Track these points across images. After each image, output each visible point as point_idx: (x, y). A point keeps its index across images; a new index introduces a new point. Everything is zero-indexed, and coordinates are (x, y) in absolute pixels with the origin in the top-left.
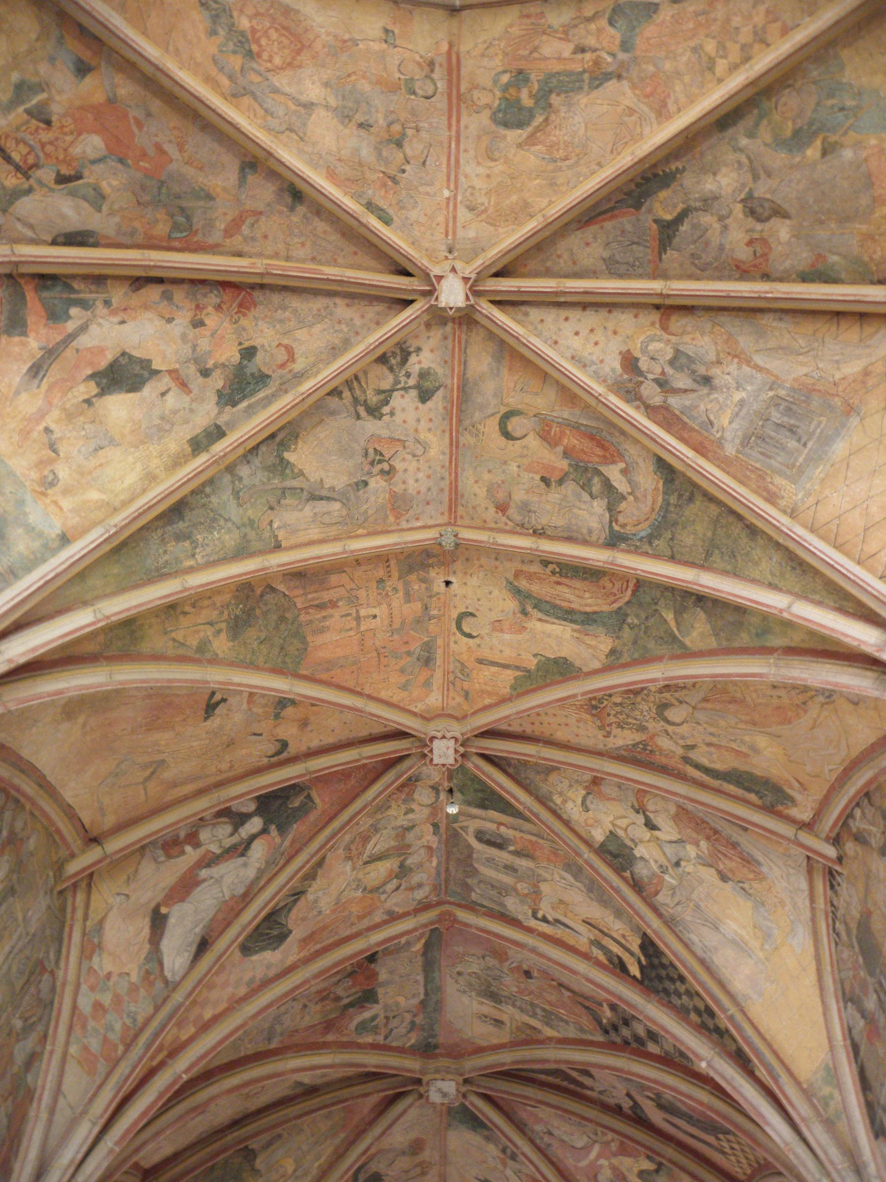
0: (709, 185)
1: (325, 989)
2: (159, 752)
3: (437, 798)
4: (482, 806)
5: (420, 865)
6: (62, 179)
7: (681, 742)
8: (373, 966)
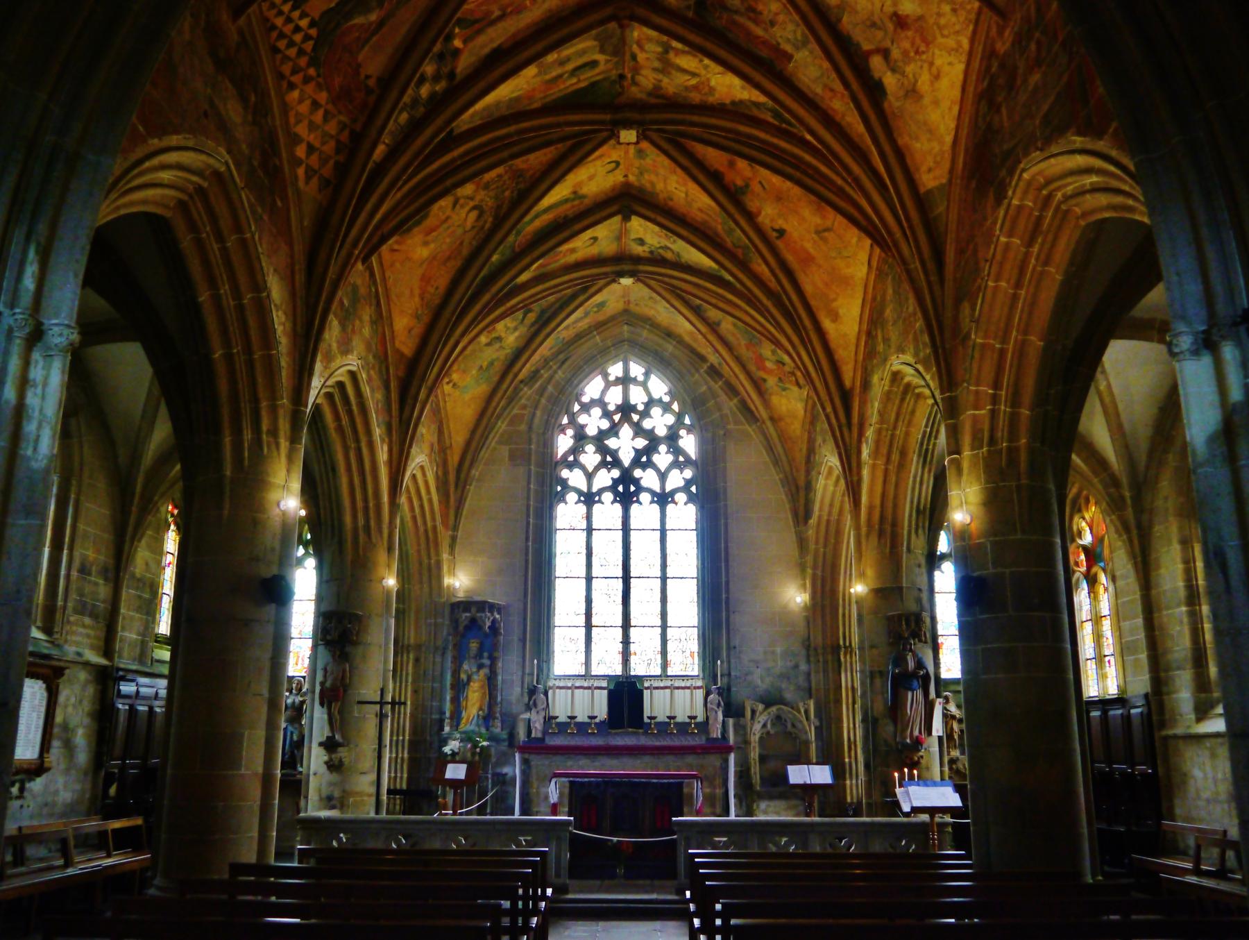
0: (517, 334)
1: (750, 18)
2: (815, 242)
3: (633, 78)
4: (593, 85)
5: (650, 39)
6: (784, 364)
7: (462, 201)
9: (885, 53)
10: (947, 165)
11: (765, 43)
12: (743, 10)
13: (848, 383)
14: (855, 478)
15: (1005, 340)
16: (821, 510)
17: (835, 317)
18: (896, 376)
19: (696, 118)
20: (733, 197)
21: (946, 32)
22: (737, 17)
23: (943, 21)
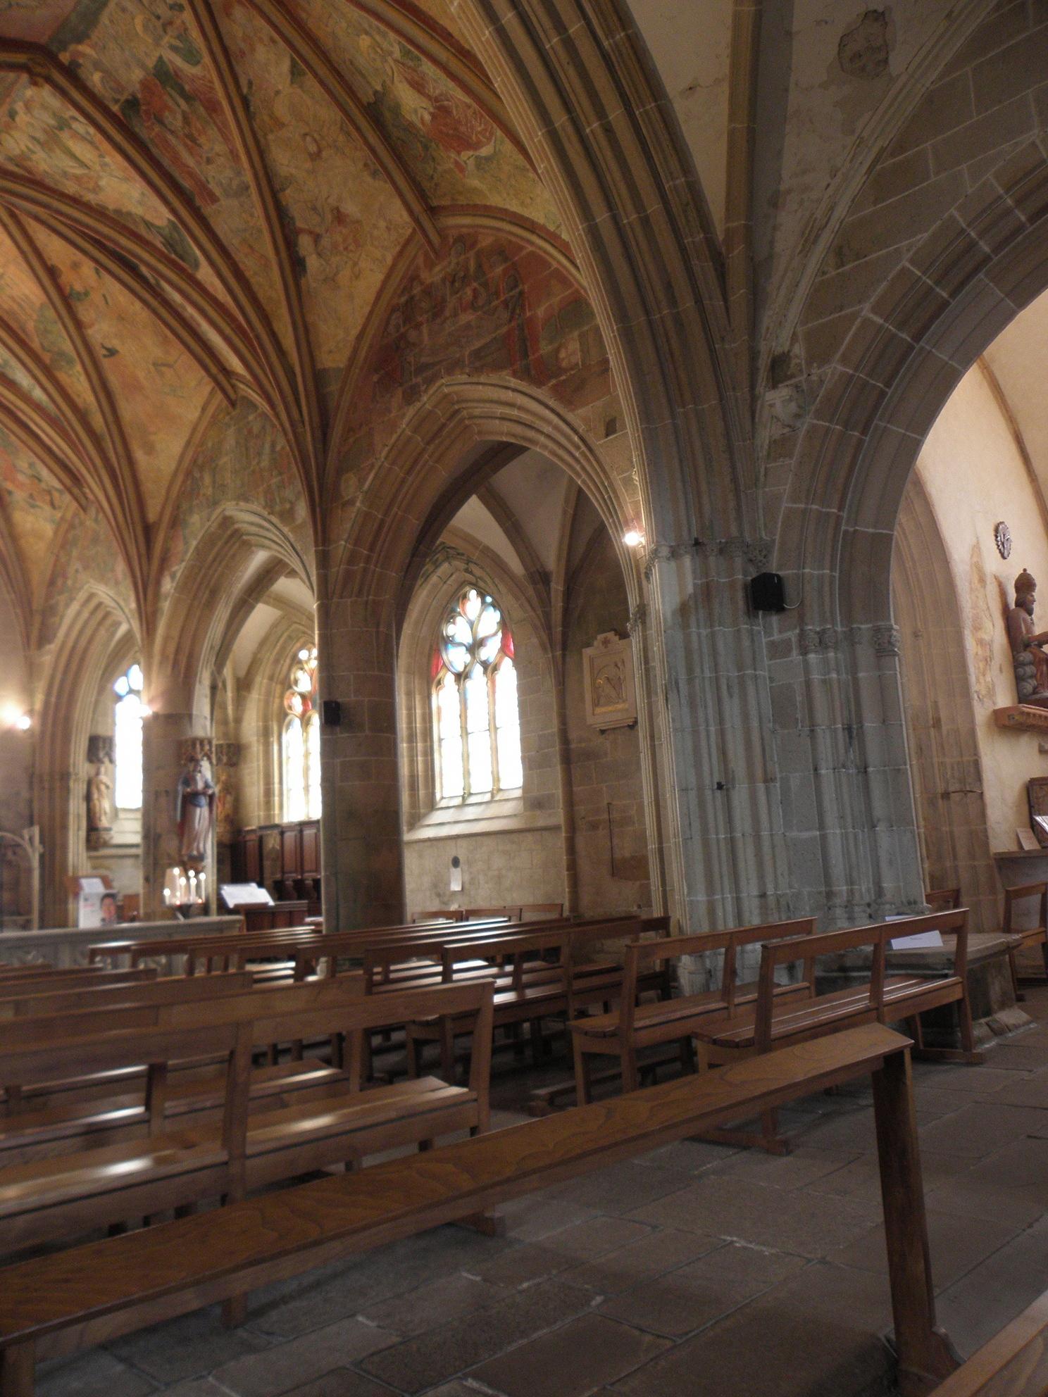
1: (186, 145)
5: (44, 107)
6: (40, 480)
8: (139, 96)
9: (317, 238)
10: (347, 353)
11: (191, 175)
12: (181, 134)
13: (152, 516)
14: (149, 609)
15: (386, 513)
16: (67, 635)
17: (150, 449)
18: (226, 521)
19: (56, 204)
20: (66, 300)
21: (376, 243)
22: (170, 137)
23: (376, 233)
